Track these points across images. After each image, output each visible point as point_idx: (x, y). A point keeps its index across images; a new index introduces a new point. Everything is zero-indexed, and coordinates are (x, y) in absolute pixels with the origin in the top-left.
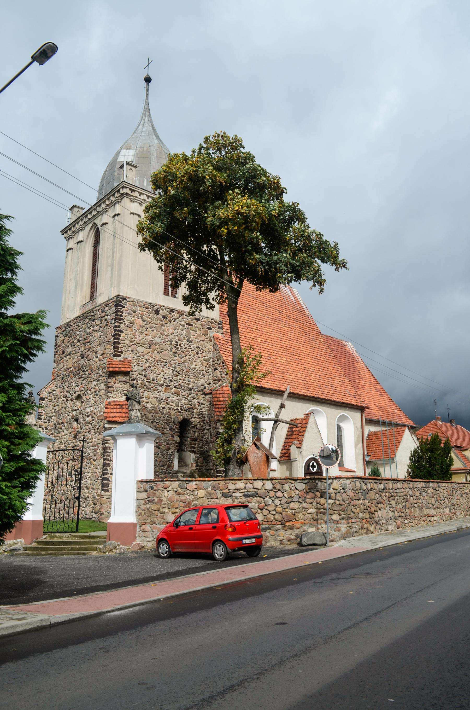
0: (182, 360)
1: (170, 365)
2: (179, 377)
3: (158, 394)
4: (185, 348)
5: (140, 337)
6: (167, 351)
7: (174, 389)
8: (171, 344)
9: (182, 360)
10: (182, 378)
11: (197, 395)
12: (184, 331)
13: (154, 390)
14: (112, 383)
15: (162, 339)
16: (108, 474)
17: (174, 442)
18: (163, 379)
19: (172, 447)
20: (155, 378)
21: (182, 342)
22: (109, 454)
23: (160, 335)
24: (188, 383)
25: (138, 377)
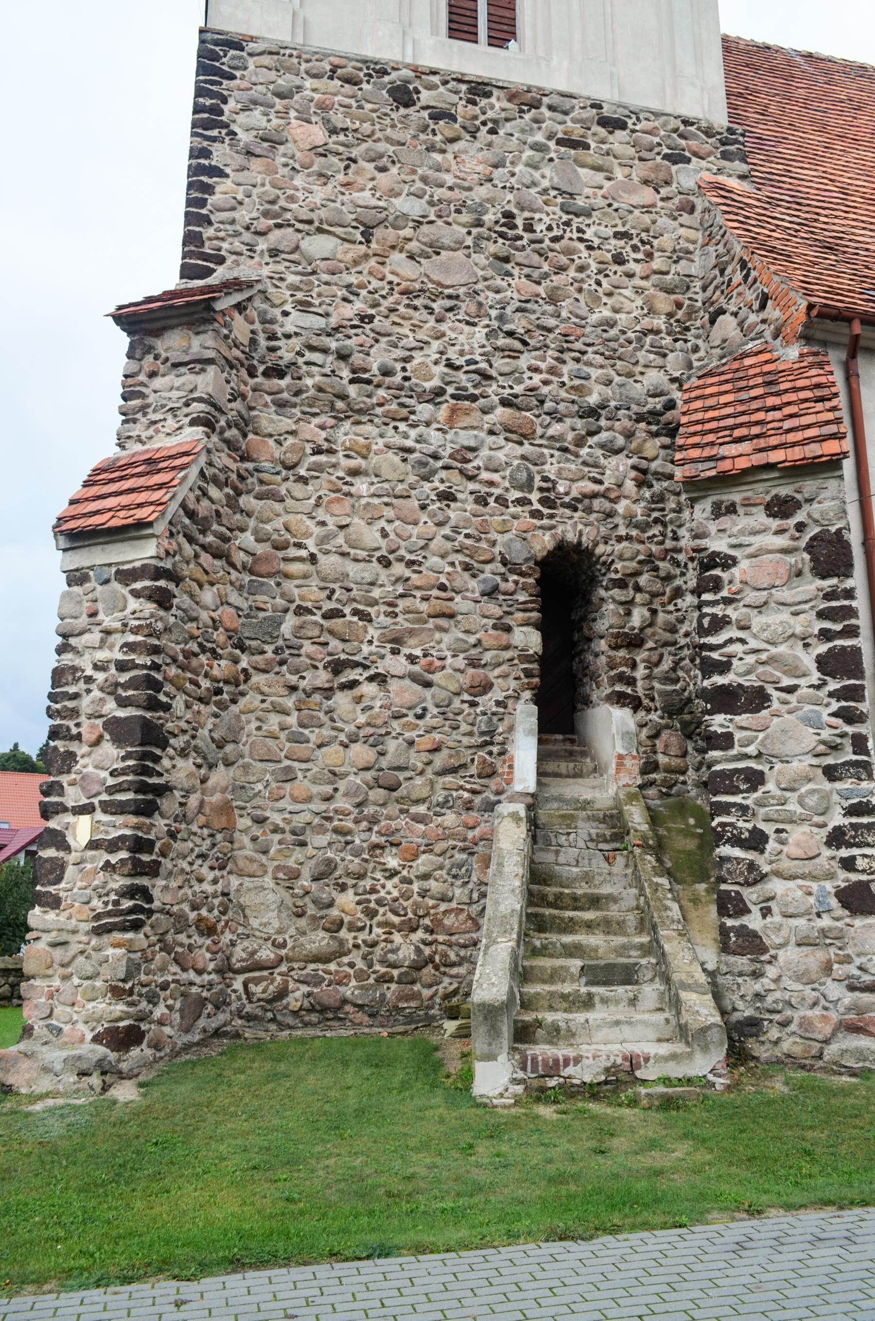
0: (541, 290)
1: (473, 309)
2: (524, 361)
3: (413, 433)
5: (311, 195)
6: (460, 254)
7: (500, 410)
8: (479, 224)
9: (541, 290)
10: (543, 366)
11: (629, 435)
14: (142, 378)
15: (431, 203)
16: (65, 810)
17: (508, 654)
18: (441, 368)
19: (505, 676)
20: (398, 366)
21: (537, 216)
22: (70, 704)
23: (419, 184)
24: (577, 382)
25: (300, 361)
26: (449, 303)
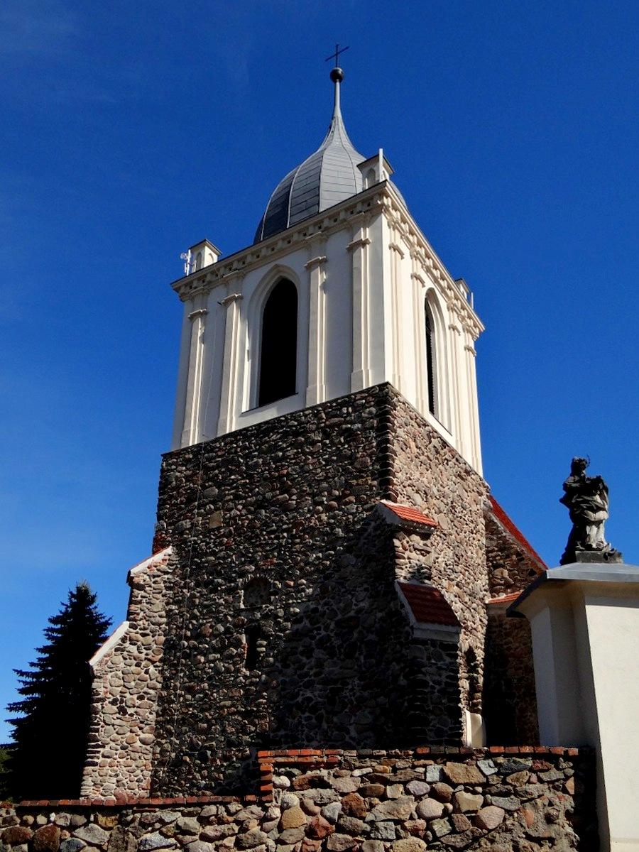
4: (461, 517)
18: (443, 565)
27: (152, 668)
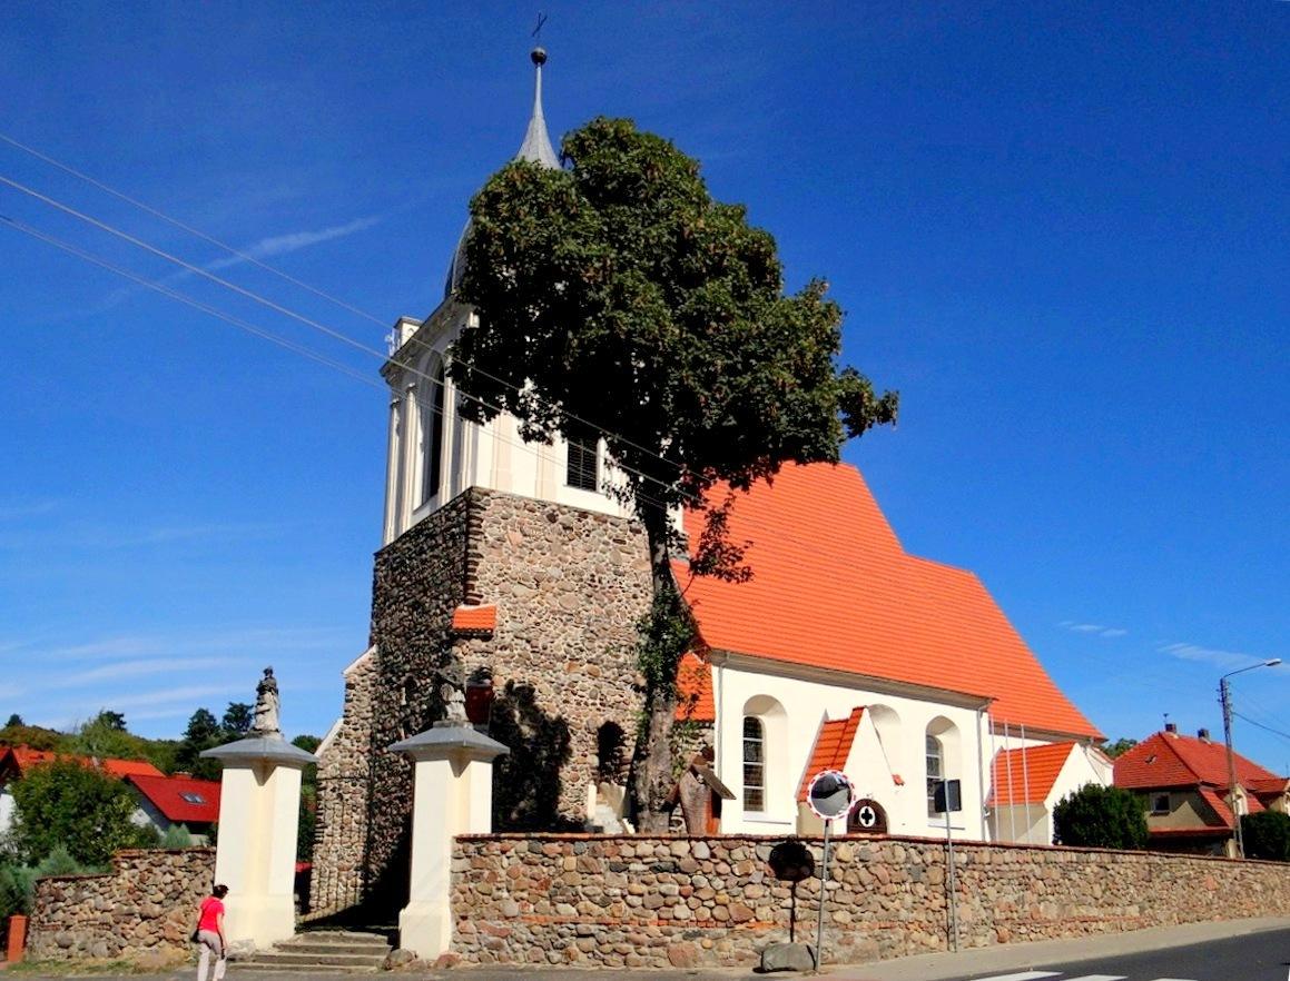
2: (596, 644)
3: (555, 675)
4: (610, 587)
5: (517, 567)
6: (573, 593)
8: (582, 580)
12: (608, 554)
13: (547, 668)
20: (549, 645)
23: (558, 561)
26: (569, 617)
27: (362, 758)
